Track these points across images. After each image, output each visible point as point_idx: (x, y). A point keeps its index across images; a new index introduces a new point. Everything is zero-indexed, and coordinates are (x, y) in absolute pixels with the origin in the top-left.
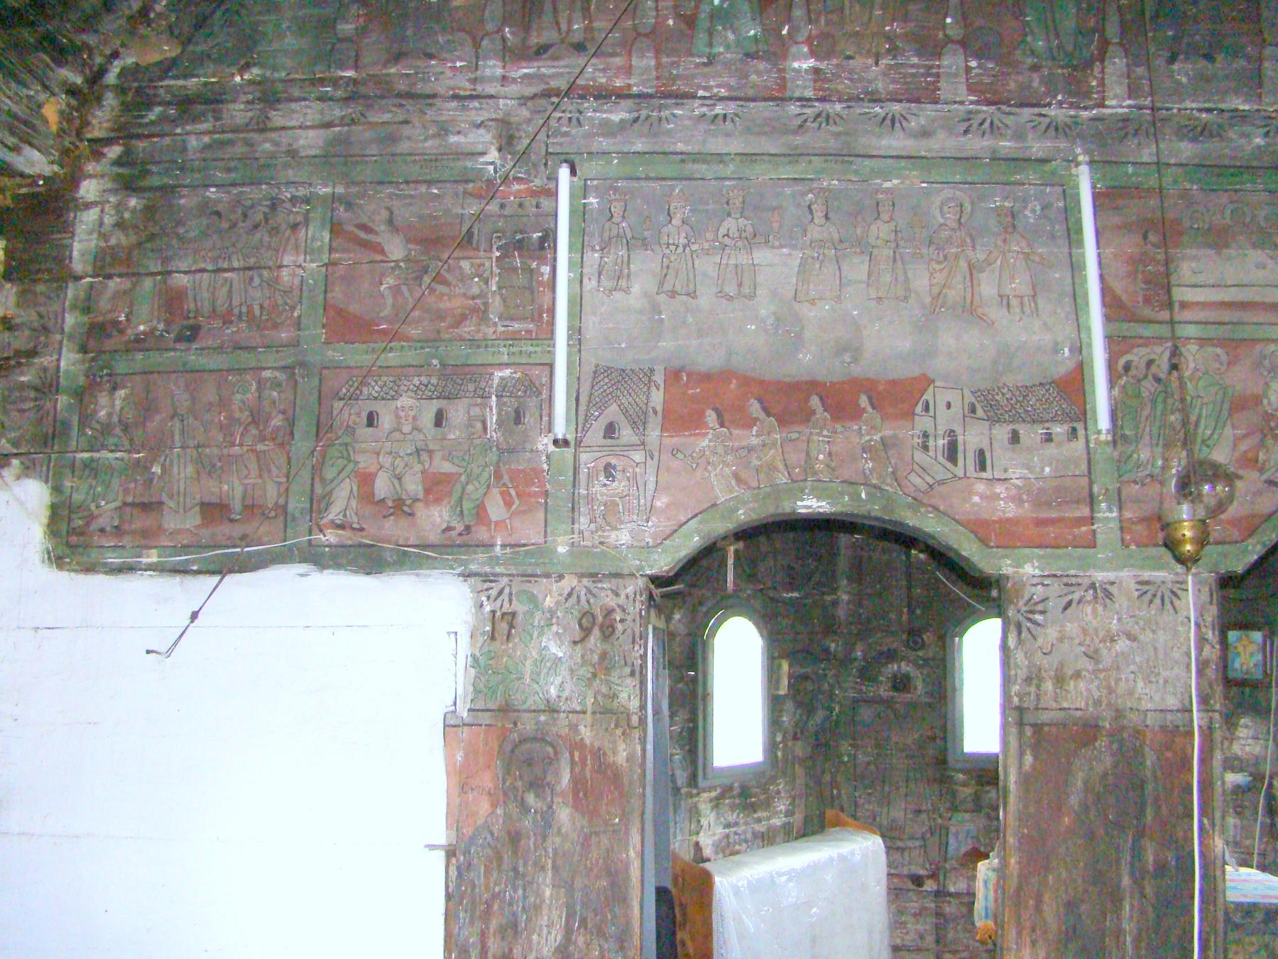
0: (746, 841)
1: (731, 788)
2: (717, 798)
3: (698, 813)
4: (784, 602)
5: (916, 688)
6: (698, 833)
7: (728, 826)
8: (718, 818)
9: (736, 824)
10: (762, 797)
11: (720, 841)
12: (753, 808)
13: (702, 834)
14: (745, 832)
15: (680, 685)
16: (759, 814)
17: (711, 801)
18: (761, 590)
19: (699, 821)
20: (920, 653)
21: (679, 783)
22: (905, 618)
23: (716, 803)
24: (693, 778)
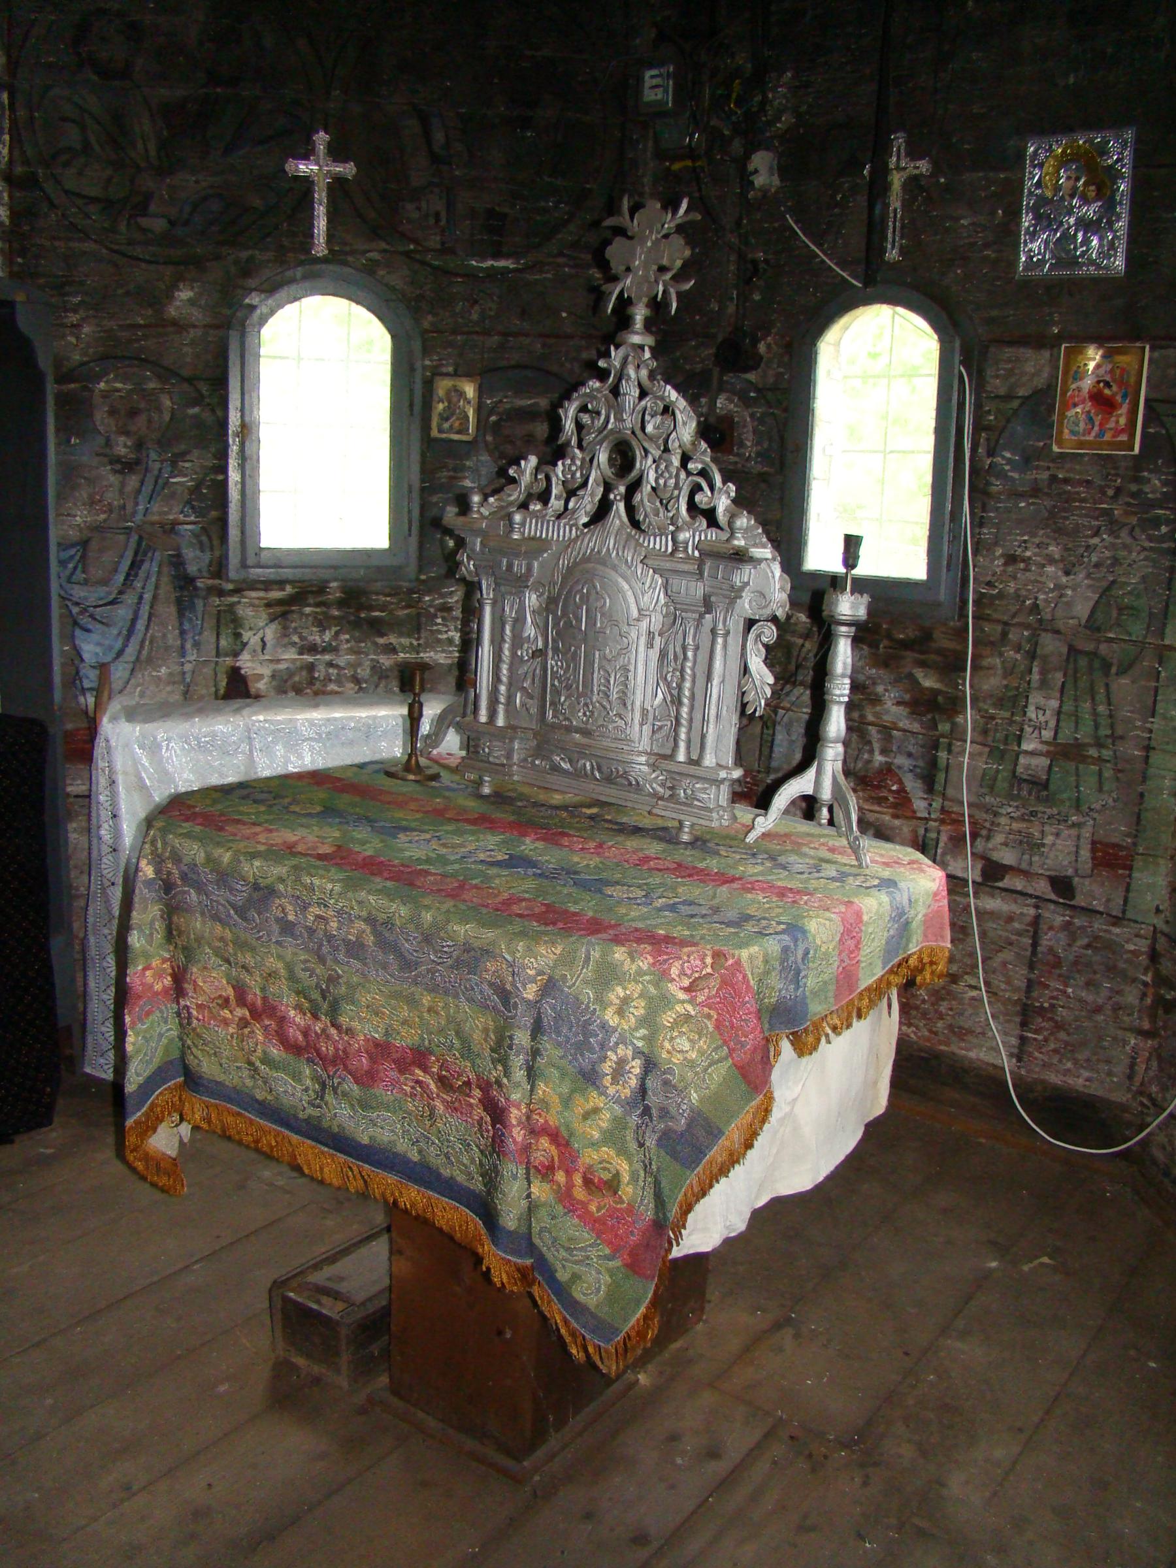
0: (356, 680)
1: (321, 589)
2: (280, 602)
3: (237, 622)
4: (471, 276)
5: (741, 445)
6: (236, 654)
7: (312, 649)
8: (285, 633)
9: (328, 649)
10: (402, 613)
11: (290, 673)
12: (377, 627)
13: (245, 656)
14: (354, 666)
15: (195, 410)
16: (393, 639)
17: (268, 605)
18: (407, 254)
19: (238, 636)
20: (751, 376)
21: (192, 569)
22: (731, 309)
23: (282, 611)
24: (219, 568)
